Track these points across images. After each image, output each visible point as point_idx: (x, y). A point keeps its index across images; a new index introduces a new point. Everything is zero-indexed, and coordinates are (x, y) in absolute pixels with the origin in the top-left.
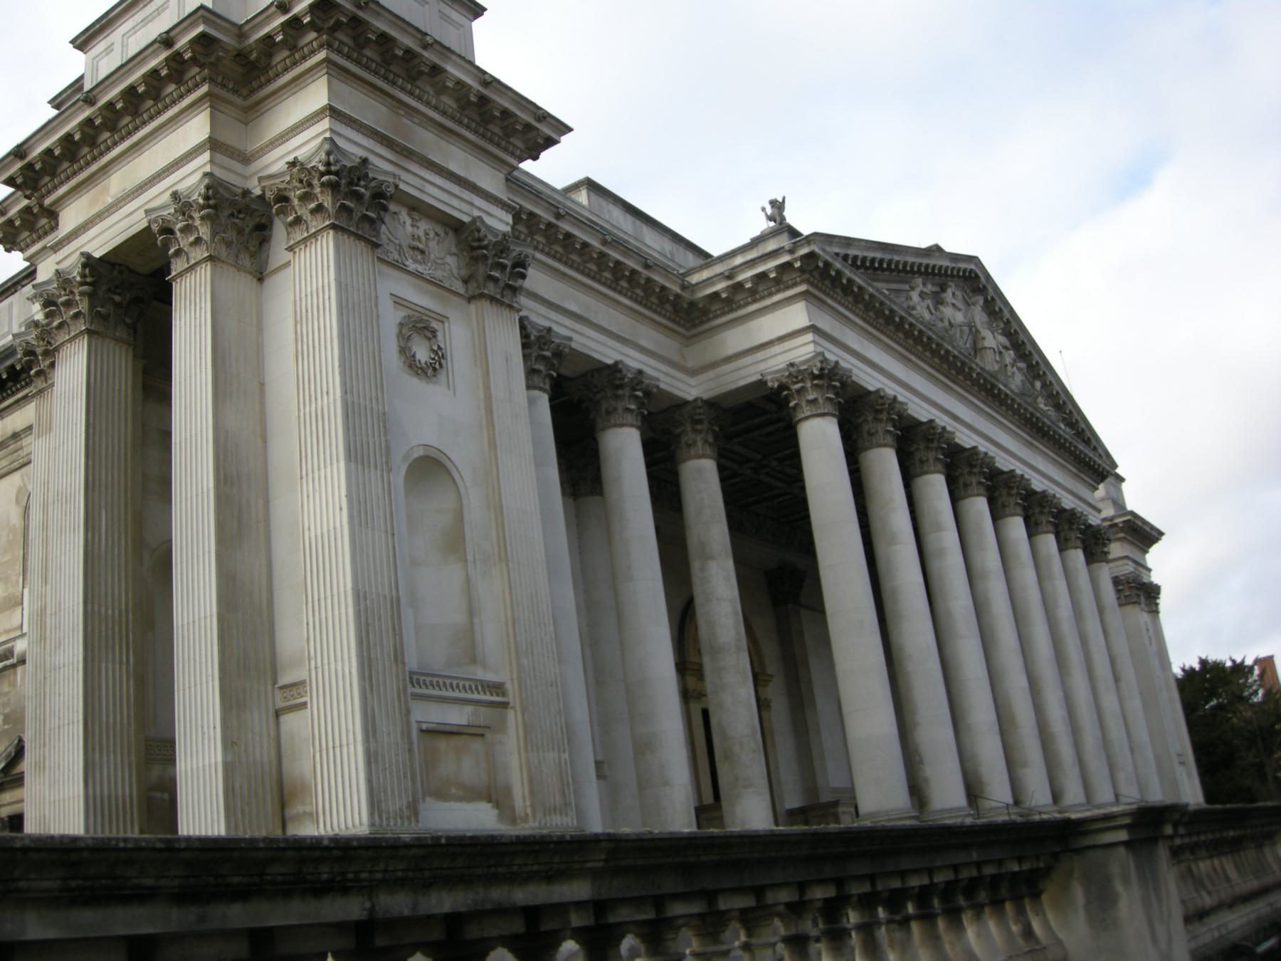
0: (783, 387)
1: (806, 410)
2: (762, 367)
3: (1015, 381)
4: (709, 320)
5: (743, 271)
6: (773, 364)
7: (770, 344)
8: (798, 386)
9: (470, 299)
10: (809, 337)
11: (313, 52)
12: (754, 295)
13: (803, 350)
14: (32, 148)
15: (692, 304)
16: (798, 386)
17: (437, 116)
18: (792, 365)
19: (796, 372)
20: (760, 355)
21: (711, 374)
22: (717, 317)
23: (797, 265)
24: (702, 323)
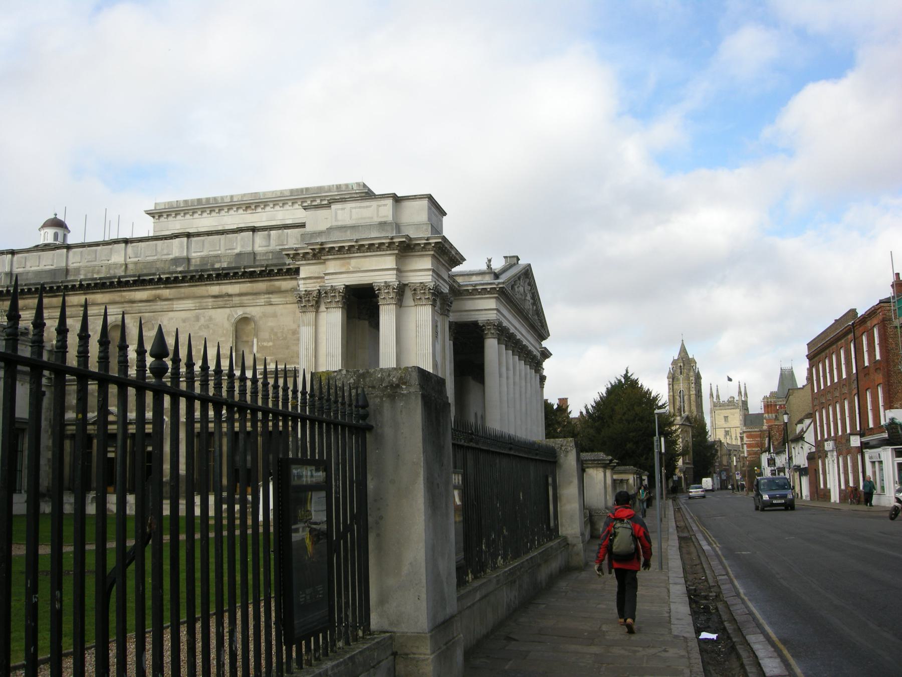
0: (484, 326)
1: (490, 336)
2: (477, 317)
3: (528, 305)
4: (461, 296)
5: (479, 286)
6: (482, 318)
7: (482, 310)
8: (489, 327)
9: (441, 314)
10: (495, 312)
11: (429, 251)
12: (480, 293)
13: (492, 316)
14: (327, 244)
15: (459, 291)
16: (489, 327)
17: (443, 262)
18: (488, 320)
19: (489, 323)
20: (477, 313)
21: (458, 314)
22: (465, 296)
23: (498, 289)
24: (459, 296)
